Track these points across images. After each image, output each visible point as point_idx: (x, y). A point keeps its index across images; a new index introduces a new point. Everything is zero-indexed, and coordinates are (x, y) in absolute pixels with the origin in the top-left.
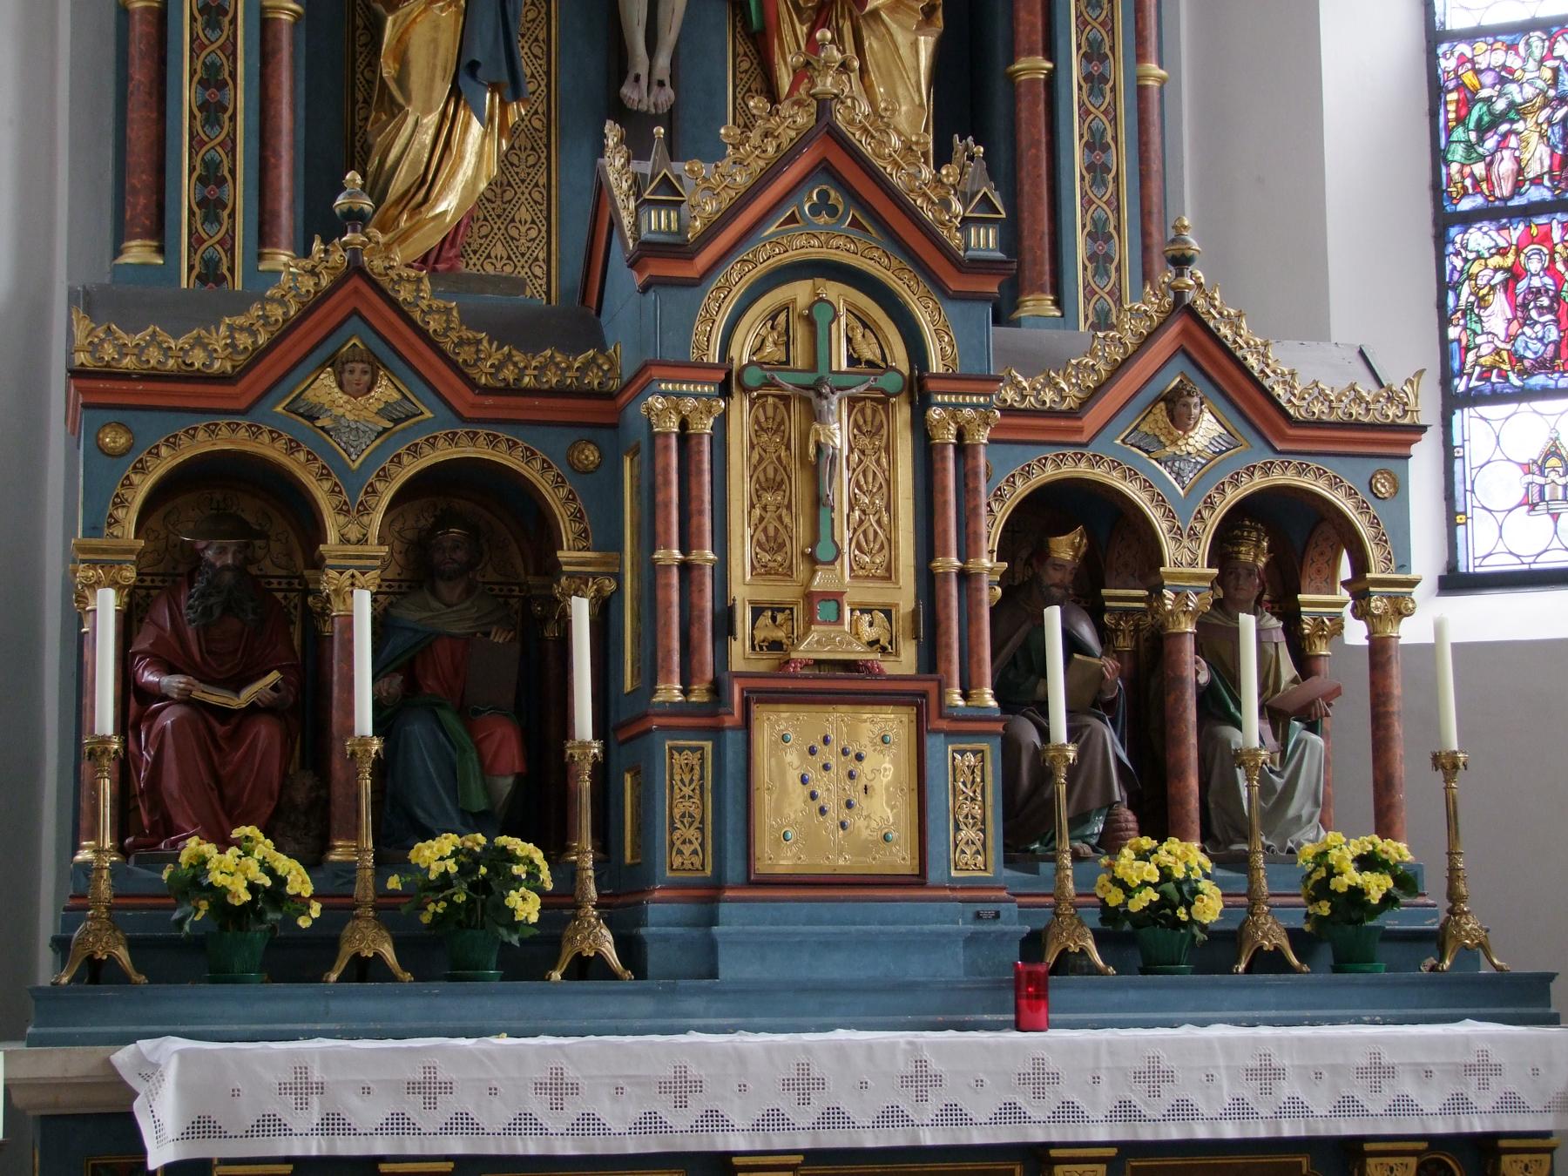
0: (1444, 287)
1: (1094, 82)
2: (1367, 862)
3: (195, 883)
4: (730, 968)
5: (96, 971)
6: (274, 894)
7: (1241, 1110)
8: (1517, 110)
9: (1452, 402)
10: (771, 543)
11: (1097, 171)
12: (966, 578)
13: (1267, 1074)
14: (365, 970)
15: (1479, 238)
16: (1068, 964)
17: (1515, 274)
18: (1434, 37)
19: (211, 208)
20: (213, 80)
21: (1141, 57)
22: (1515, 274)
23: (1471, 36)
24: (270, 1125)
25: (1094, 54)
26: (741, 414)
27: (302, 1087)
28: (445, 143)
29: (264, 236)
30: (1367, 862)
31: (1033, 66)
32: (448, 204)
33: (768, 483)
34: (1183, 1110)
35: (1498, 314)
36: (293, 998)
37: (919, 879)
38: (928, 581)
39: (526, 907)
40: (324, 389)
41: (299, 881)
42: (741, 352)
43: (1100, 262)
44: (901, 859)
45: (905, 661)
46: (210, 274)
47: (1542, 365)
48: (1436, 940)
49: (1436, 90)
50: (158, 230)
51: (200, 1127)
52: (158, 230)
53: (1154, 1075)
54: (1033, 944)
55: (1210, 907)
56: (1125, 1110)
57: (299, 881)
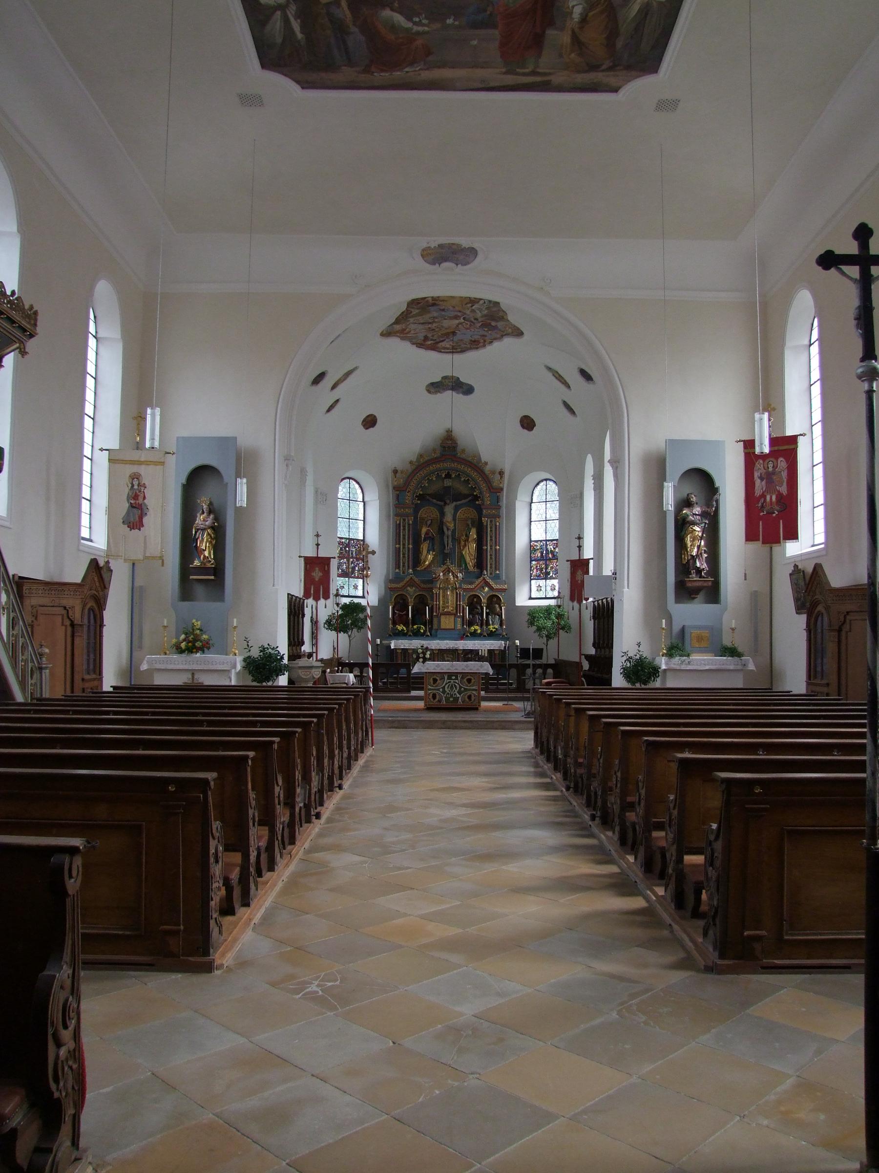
0: (531, 567)
1: (491, 549)
2: (493, 628)
3: (397, 629)
4: (438, 636)
5: (390, 635)
6: (403, 630)
7: (472, 647)
8: (538, 550)
9: (531, 579)
10: (444, 601)
11: (491, 558)
12: (460, 604)
13: (475, 644)
14: (410, 636)
15: (534, 563)
16: (468, 636)
17: (537, 567)
18: (531, 541)
19: (404, 566)
20: (404, 554)
21: (496, 546)
22: (537, 567)
23: (534, 541)
24: (400, 646)
25: (491, 546)
26: (441, 591)
27: (402, 643)
28: (426, 556)
29: (409, 568)
30: (494, 628)
31: (485, 548)
32: (427, 563)
33: (443, 597)
34: (468, 647)
35: (535, 570)
36: (405, 637)
37: (454, 629)
38: (457, 605)
39: (422, 631)
40: (409, 588)
41: (405, 629)
42: (441, 586)
43: (491, 567)
44: (453, 627)
45: (455, 611)
46: (404, 573)
47: (539, 576)
48: (500, 634)
49: (531, 546)
50: (399, 568)
51: (395, 646)
52: (399, 568)
53: (465, 644)
54: (464, 634)
55: (479, 631)
56: (463, 647)
57: (405, 629)
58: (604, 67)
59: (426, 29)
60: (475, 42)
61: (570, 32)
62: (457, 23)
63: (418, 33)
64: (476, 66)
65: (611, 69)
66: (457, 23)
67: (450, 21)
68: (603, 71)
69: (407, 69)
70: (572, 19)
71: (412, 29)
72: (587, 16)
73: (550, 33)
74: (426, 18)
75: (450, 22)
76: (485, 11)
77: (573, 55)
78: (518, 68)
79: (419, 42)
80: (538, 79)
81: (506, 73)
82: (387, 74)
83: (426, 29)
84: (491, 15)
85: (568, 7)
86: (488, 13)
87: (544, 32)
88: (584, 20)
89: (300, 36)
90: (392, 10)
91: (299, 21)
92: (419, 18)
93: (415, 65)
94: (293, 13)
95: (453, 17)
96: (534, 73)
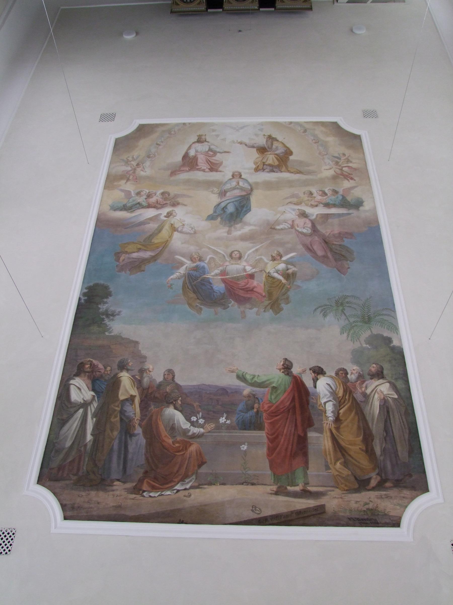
58: (373, 483)
59: (202, 430)
60: (244, 447)
61: (329, 434)
62: (228, 422)
63: (194, 436)
64: (246, 483)
65: (380, 486)
66: (228, 422)
67: (222, 420)
68: (373, 489)
69: (178, 487)
70: (327, 417)
71: (190, 430)
72: (339, 414)
73: (312, 435)
74: (203, 417)
75: (223, 421)
76: (253, 408)
77: (338, 465)
78: (288, 486)
79: (193, 448)
80: (310, 503)
81: (277, 493)
82: (157, 495)
83: (202, 430)
84: (258, 412)
85: (321, 404)
86: (255, 410)
87: (306, 435)
88: (337, 420)
89: (89, 437)
90: (176, 408)
91: (95, 419)
92: (197, 417)
93: (187, 481)
94: (93, 410)
95: (225, 415)
96: (305, 494)
